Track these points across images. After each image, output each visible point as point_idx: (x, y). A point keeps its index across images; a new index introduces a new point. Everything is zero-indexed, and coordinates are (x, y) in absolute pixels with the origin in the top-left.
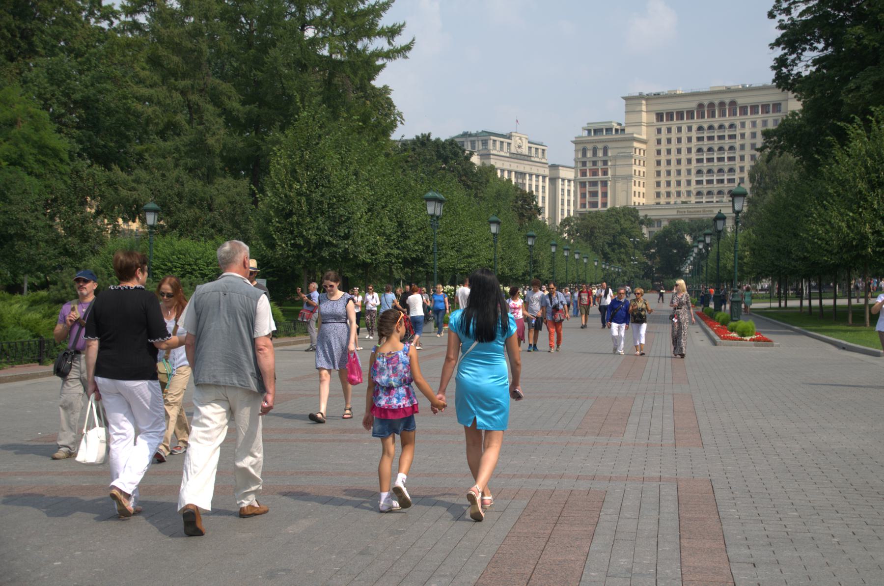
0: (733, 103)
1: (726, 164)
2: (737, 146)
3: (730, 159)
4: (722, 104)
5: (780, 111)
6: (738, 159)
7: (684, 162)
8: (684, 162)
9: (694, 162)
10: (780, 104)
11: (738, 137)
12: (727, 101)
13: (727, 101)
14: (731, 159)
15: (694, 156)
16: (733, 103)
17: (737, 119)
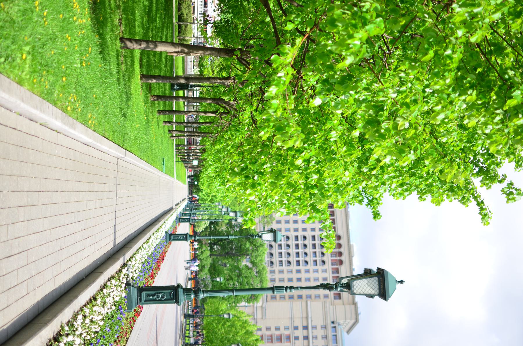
0: (341, 262)
1: (293, 259)
2: (308, 267)
3: (298, 262)
4: (340, 254)
5: (335, 298)
6: (298, 268)
7: (296, 226)
8: (296, 226)
9: (296, 234)
10: (340, 298)
11: (316, 268)
12: (342, 258)
13: (342, 258)
14: (298, 262)
15: (300, 234)
16: (341, 262)
17: (329, 266)
